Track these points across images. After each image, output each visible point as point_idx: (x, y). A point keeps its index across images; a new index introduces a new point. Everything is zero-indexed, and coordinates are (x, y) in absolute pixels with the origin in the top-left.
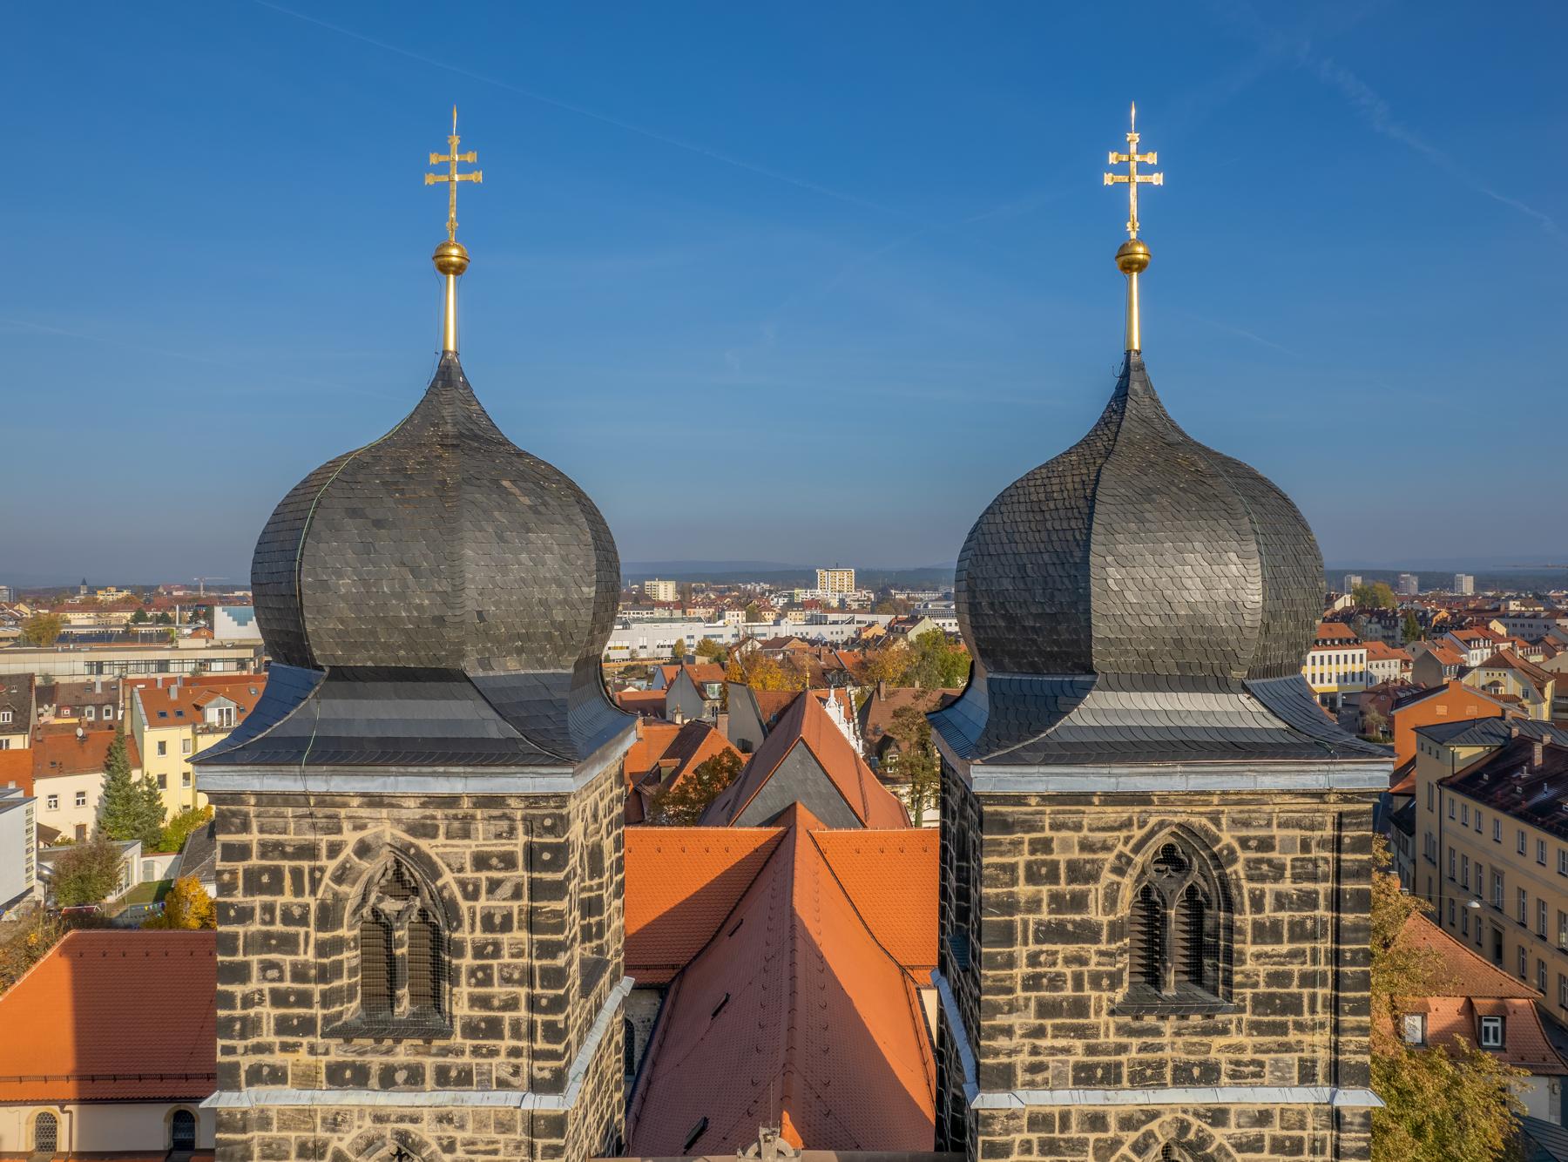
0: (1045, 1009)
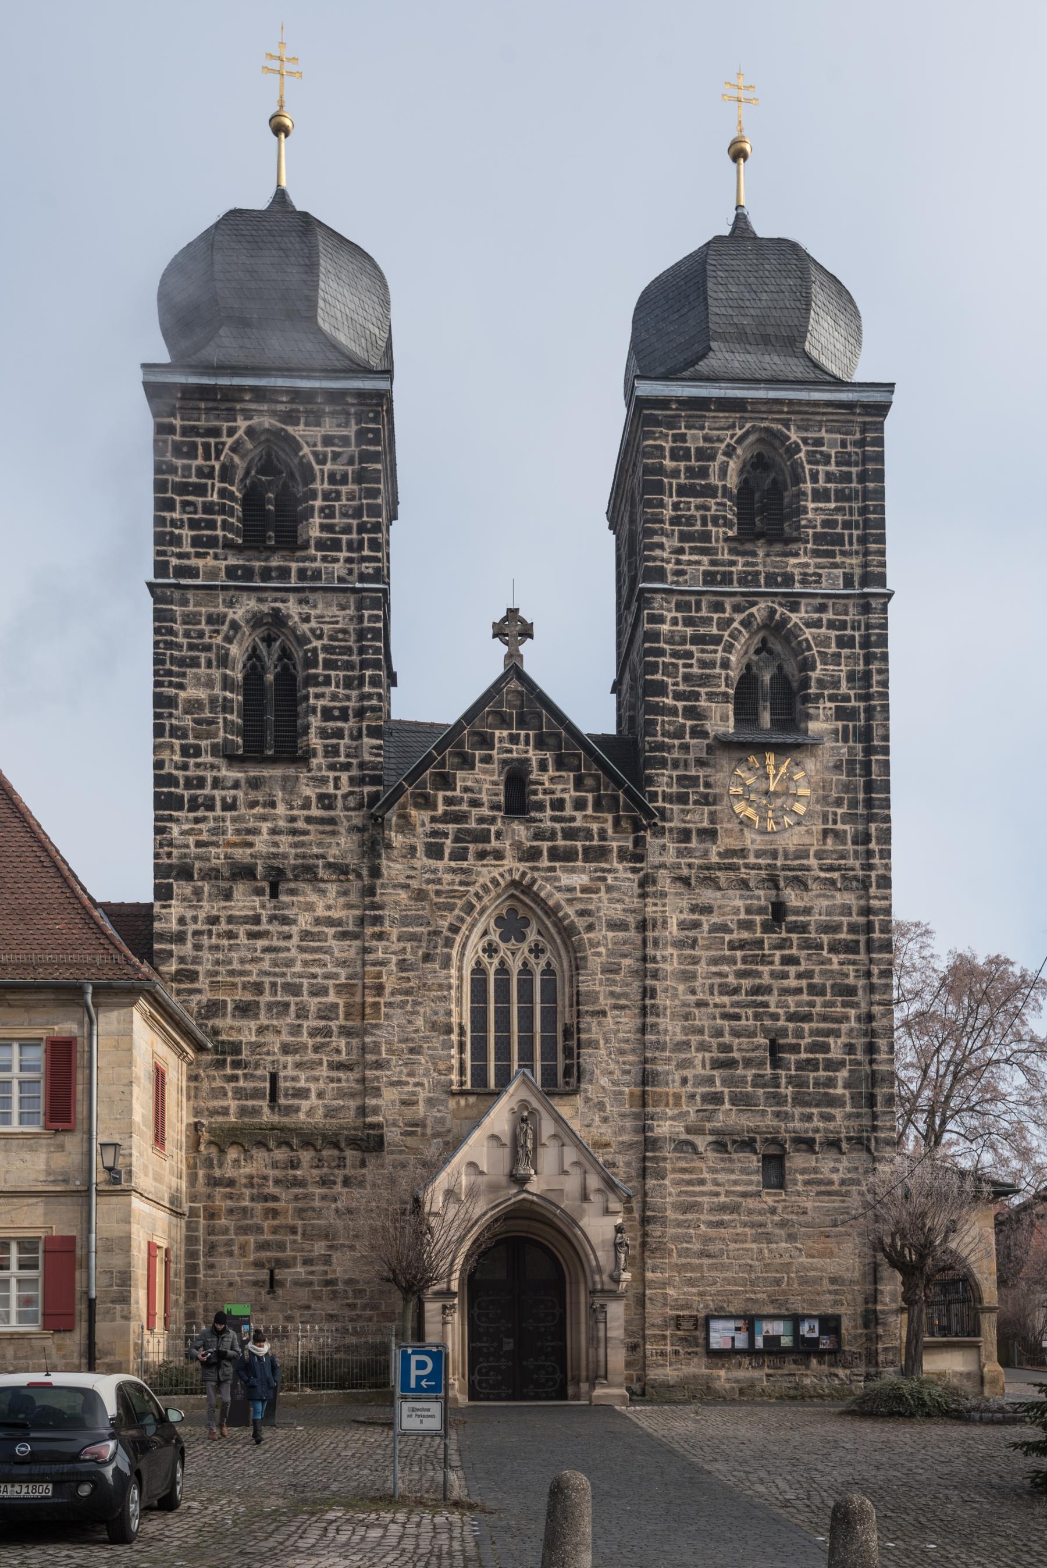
0: (684, 537)
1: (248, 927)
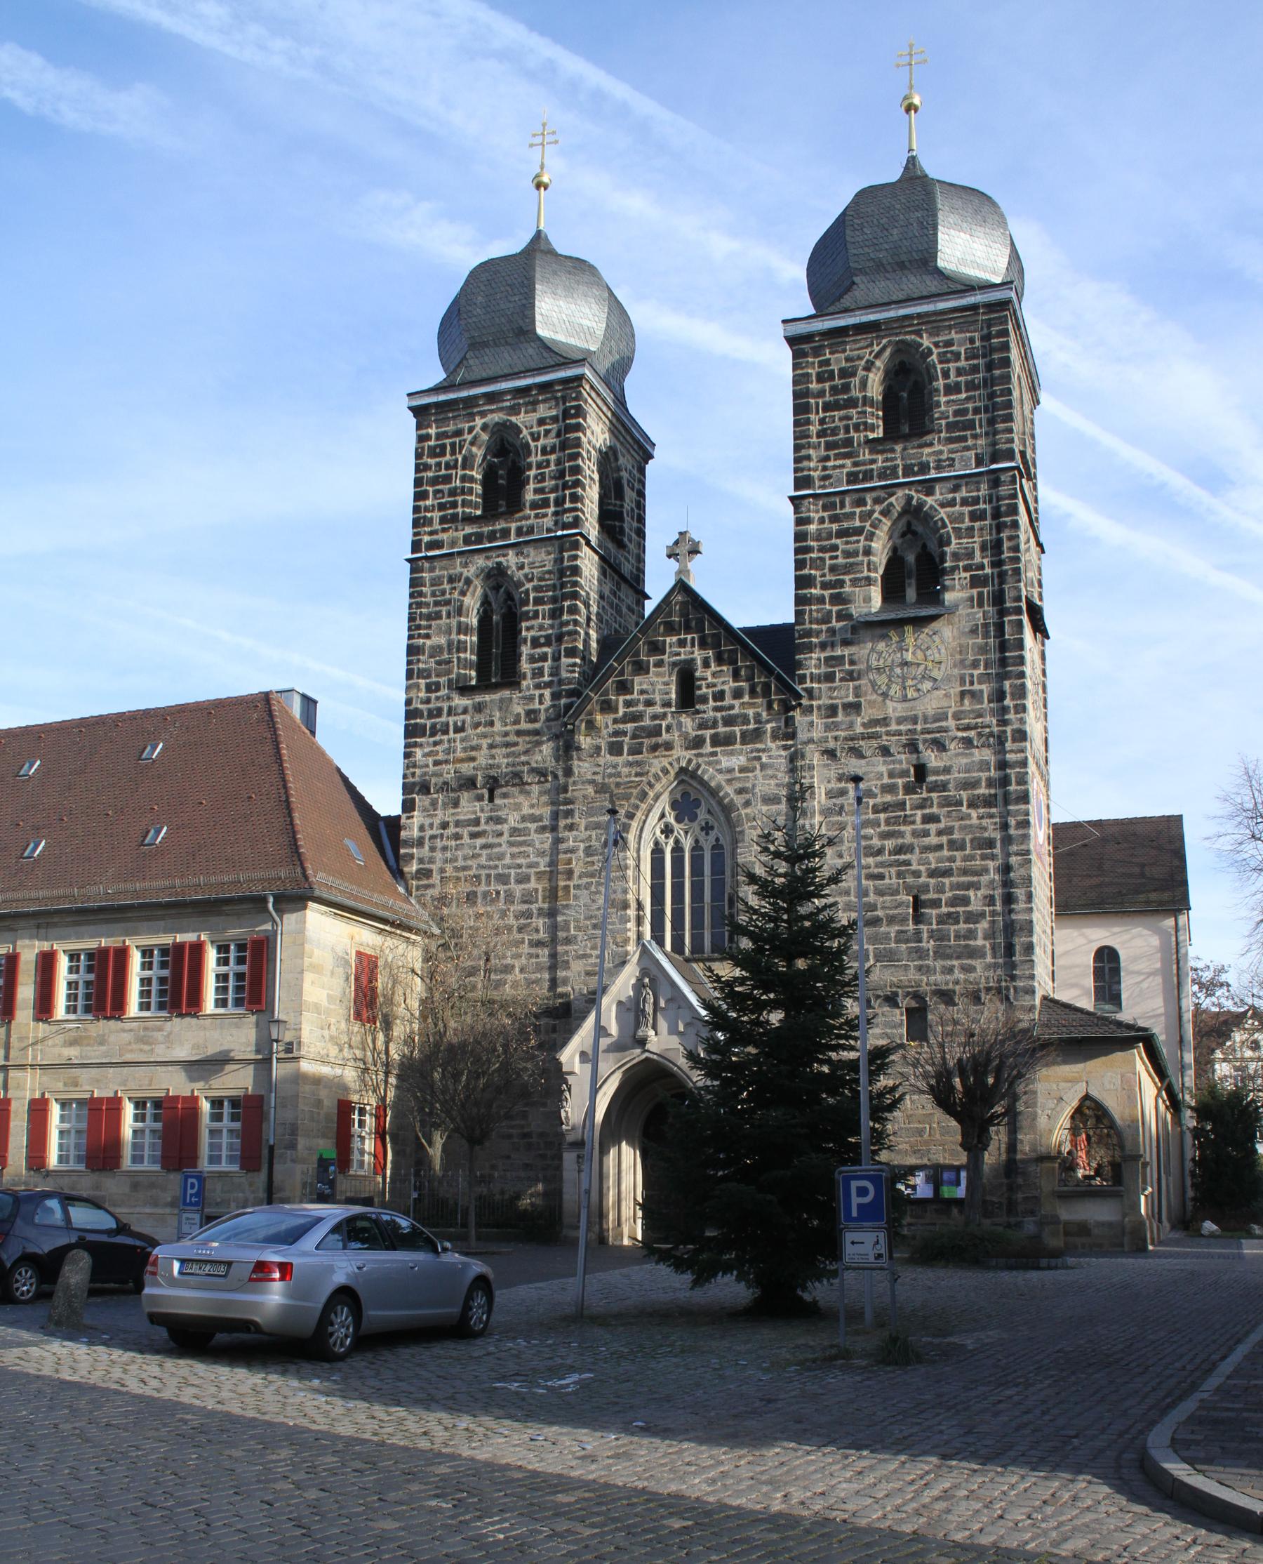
0: (829, 446)
1: (471, 828)
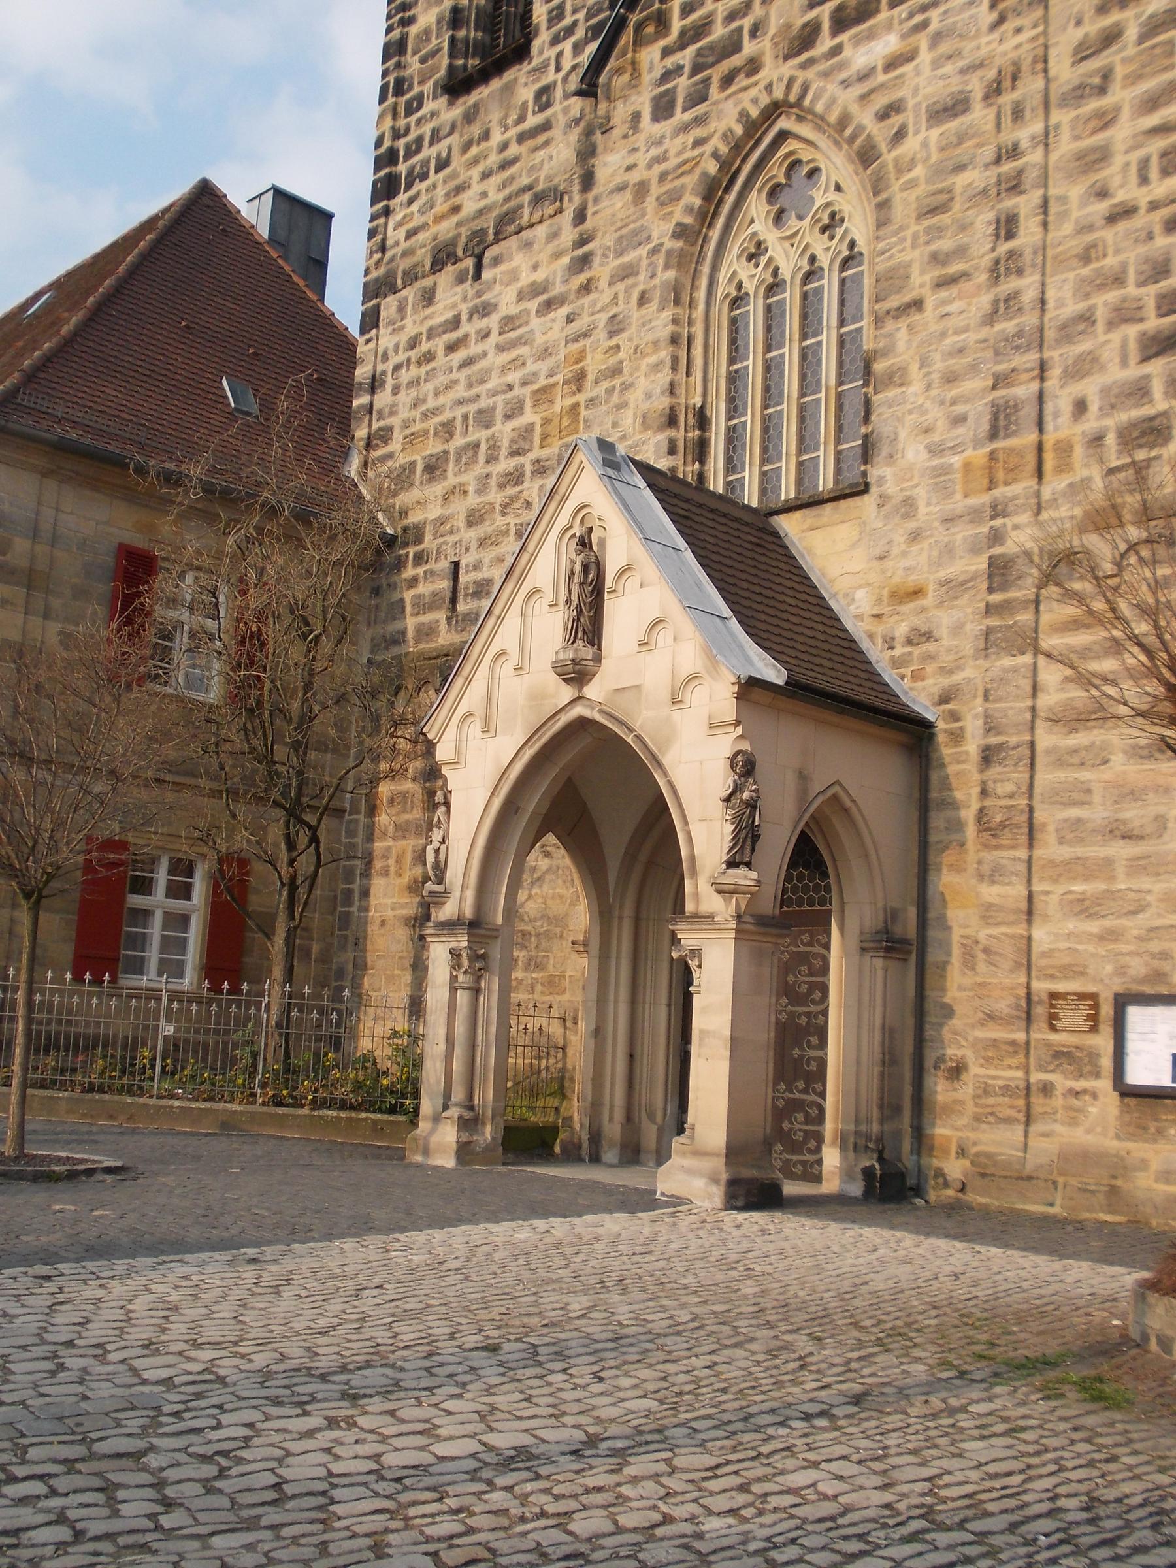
1: (446, 337)
